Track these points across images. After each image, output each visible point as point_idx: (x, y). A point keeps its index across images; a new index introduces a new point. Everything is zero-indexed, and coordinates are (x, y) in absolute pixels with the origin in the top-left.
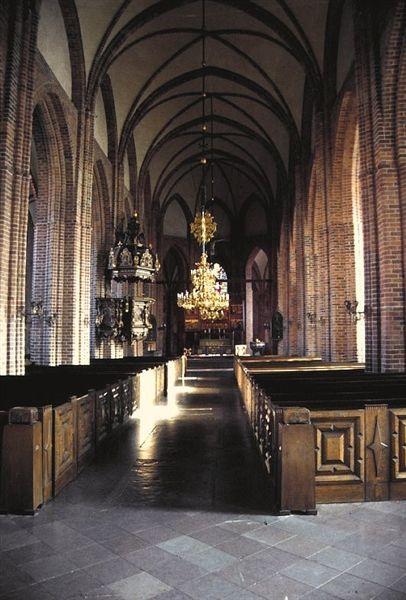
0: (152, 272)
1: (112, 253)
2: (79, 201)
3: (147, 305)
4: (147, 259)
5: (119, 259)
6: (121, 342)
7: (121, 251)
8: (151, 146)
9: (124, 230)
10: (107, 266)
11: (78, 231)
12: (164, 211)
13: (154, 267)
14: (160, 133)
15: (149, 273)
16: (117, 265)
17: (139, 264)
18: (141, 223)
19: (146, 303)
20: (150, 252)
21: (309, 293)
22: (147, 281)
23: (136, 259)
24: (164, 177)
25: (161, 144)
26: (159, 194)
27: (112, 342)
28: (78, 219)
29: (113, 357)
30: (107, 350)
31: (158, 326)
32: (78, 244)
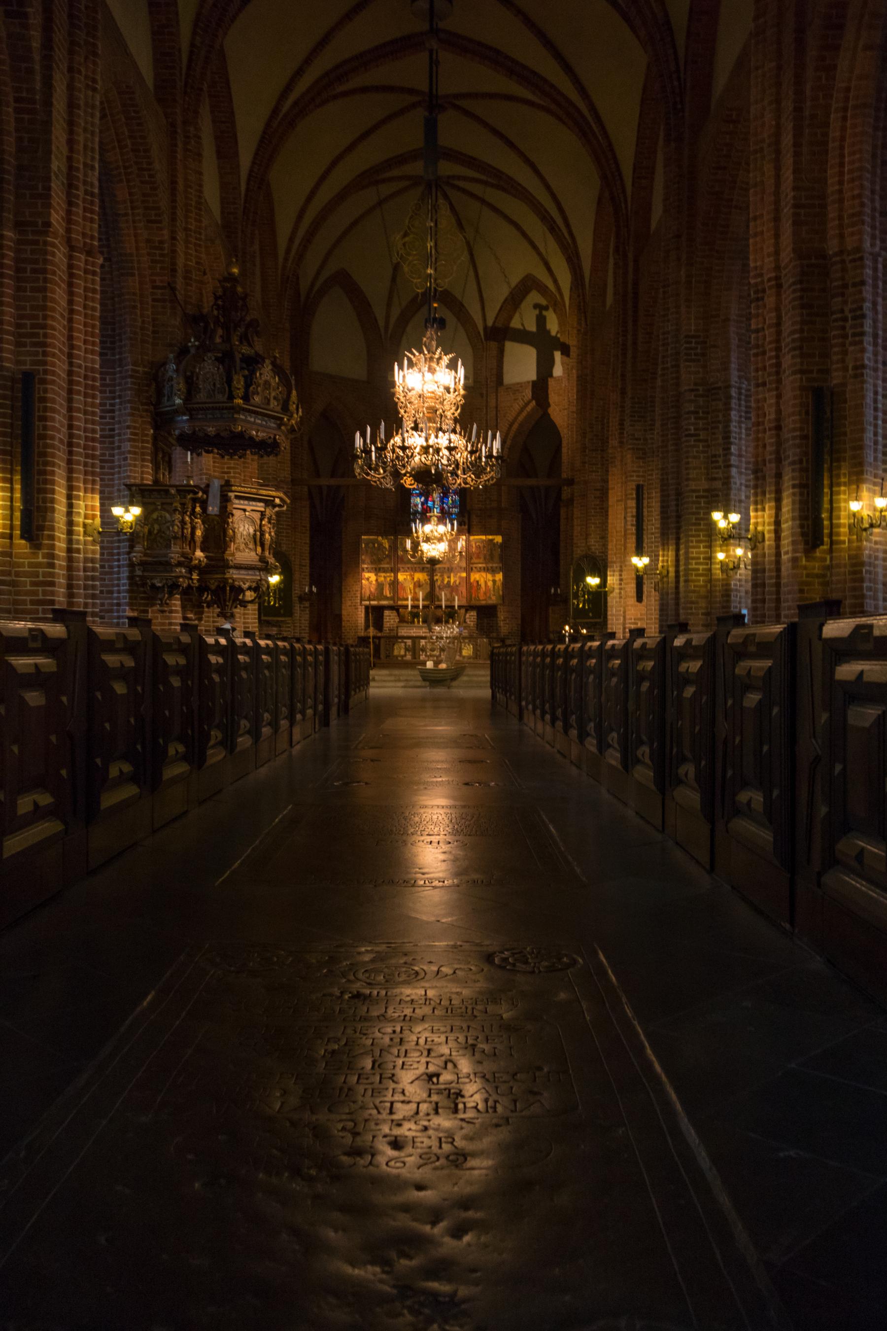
2: (57, 164)
3: (269, 512)
4: (267, 383)
8: (275, 111)
11: (59, 255)
14: (299, 72)
17: (246, 398)
20: (277, 369)
22: (267, 448)
23: (239, 382)
24: (301, 232)
28: (56, 218)
31: (296, 591)
32: (59, 295)
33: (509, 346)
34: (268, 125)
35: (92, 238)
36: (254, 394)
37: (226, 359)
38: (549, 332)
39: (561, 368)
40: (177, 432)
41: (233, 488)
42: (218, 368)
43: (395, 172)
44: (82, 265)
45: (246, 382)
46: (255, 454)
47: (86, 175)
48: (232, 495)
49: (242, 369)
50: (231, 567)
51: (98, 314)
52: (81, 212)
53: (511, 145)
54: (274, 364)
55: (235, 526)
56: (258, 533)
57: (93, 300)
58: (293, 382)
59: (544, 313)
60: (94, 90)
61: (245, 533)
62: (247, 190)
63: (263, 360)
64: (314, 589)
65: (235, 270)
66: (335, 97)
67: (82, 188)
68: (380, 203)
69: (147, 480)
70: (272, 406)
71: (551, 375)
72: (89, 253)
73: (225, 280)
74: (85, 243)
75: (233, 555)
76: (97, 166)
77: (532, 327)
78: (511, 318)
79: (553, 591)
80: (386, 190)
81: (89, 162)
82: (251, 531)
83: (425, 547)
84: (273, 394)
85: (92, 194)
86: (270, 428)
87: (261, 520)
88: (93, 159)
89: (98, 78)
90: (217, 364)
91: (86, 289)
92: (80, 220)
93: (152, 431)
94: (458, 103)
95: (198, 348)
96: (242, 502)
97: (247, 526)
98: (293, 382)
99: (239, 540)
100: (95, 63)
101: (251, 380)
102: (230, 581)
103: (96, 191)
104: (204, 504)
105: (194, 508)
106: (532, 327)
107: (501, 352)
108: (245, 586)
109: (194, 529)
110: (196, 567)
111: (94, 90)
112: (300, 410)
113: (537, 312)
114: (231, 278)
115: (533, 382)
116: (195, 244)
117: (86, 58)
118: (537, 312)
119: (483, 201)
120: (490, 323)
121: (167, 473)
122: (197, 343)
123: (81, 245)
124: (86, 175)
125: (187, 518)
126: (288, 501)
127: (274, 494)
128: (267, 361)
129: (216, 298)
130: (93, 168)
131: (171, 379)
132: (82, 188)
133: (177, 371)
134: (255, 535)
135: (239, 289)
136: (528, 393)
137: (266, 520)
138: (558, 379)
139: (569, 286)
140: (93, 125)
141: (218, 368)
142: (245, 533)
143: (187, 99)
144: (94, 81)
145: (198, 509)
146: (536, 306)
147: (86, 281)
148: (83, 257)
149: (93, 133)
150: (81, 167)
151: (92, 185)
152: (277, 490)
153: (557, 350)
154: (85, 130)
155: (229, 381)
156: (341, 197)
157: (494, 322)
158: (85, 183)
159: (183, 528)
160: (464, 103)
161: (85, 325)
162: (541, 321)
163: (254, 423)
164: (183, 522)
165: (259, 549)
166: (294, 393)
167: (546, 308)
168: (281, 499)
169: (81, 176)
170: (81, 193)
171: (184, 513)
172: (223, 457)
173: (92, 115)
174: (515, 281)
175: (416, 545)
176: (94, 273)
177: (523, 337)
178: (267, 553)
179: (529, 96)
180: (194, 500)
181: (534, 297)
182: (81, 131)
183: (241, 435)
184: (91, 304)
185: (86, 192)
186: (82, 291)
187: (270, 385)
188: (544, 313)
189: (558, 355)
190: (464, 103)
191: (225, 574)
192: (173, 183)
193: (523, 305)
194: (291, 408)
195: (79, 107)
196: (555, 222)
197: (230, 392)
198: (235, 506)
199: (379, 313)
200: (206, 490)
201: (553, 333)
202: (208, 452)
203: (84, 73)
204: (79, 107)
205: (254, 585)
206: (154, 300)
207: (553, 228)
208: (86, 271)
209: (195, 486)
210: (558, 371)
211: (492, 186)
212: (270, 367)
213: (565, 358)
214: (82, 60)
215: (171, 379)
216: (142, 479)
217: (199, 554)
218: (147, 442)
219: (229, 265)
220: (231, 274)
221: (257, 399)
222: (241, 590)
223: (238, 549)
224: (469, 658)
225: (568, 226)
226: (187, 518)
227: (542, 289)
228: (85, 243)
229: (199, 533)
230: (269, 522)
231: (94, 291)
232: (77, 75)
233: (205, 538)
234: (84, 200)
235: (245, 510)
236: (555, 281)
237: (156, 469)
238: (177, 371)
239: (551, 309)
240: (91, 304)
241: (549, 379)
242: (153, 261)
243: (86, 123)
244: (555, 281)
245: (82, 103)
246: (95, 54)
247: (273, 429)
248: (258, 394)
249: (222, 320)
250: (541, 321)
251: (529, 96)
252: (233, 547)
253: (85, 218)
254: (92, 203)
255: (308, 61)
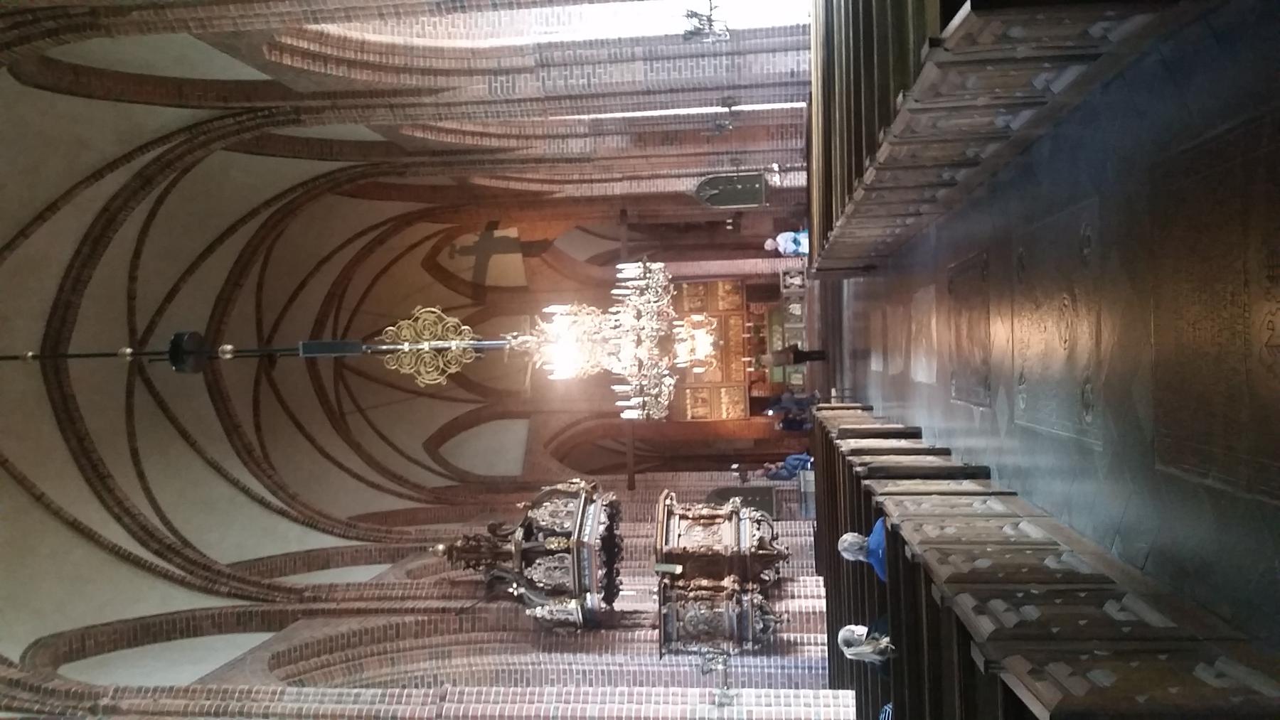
0: (589, 501)
1: (539, 612)
3: (678, 510)
5: (558, 592)
6: (779, 583)
7: (531, 584)
8: (282, 513)
9: (479, 577)
10: (574, 624)
12: (464, 478)
13: (575, 495)
14: (246, 491)
15: (591, 508)
16: (572, 596)
17: (568, 535)
18: (458, 531)
19: (670, 514)
20: (536, 505)
21: (640, 77)
22: (614, 514)
23: (553, 544)
25: (278, 488)
26: (416, 487)
27: (779, 607)
29: (822, 605)
30: (806, 618)
31: (738, 484)
33: (489, 282)
34: (295, 520)
35: (426, 695)
36: (563, 528)
37: (528, 557)
38: (476, 243)
39: (510, 229)
40: (603, 605)
41: (659, 547)
42: (539, 564)
43: (332, 397)
44: (454, 706)
45: (550, 535)
46: (617, 526)
47: (365, 702)
48: (664, 551)
49: (537, 539)
50: (739, 548)
51: (502, 689)
52: (401, 708)
53: (302, 285)
54: (532, 508)
55: (696, 544)
56: (702, 521)
57: (488, 694)
58: (548, 488)
59: (458, 247)
60: (282, 693)
61: (702, 535)
62: (357, 539)
63: (527, 518)
64: (735, 466)
65: (441, 547)
66: (266, 456)
67: (376, 707)
68: (361, 410)
69: (652, 636)
70: (573, 509)
71: (517, 239)
72: (443, 699)
73: (450, 558)
74: (432, 703)
75: (726, 548)
76: (356, 691)
77: (471, 260)
78: (463, 281)
79: (729, 227)
80: (348, 406)
81: (352, 698)
82: (699, 528)
83: (700, 355)
84: (562, 508)
85: (384, 695)
86: (595, 511)
87: (687, 518)
88: (349, 695)
89: (271, 689)
90: (534, 565)
91: (478, 702)
92: (410, 708)
93: (603, 631)
94: (266, 336)
95: (519, 585)
96: (671, 538)
97: (695, 533)
98: (548, 488)
99: (709, 542)
100: (257, 692)
101: (548, 529)
102: (753, 550)
103: (380, 691)
104: (674, 577)
105: (680, 588)
106: (471, 260)
107: (496, 289)
108: (758, 534)
109: (701, 588)
110: (740, 585)
111: (282, 693)
112: (574, 480)
113: (457, 256)
114: (449, 552)
115: (524, 255)
116: (417, 589)
117: (254, 700)
118: (457, 256)
119: (355, 312)
120: (469, 301)
121: (643, 616)
122: (515, 585)
123: (435, 707)
124: (365, 702)
125: (692, 594)
126: (666, 491)
127: (661, 505)
128: (530, 514)
129: (468, 567)
130: (358, 695)
131: (551, 612)
132: (376, 707)
133: (543, 606)
134: (704, 525)
135: (459, 543)
136: (535, 261)
137: (688, 513)
138: (520, 233)
139: (431, 225)
140: (315, 695)
141: (539, 564)
142: (702, 535)
143: (278, 599)
144: (274, 693)
145: (681, 583)
146: (451, 257)
147: (470, 702)
148: (446, 705)
149: (324, 695)
150: (357, 706)
151: (374, 696)
152: (657, 502)
153: (492, 235)
154: (321, 702)
155: (552, 552)
156: (357, 448)
157: (467, 297)
158: (373, 703)
159: (702, 599)
160: (267, 330)
161: (514, 702)
162: (465, 251)
163: (592, 526)
164: (696, 599)
165: (718, 520)
166: (559, 486)
167: (453, 246)
168: (666, 498)
169: (366, 707)
170: (383, 707)
171: (686, 599)
172: (622, 558)
173: (307, 695)
174: (428, 278)
175: (701, 363)
176: (462, 693)
177: (481, 268)
178: (720, 512)
179: (256, 269)
180: (672, 587)
181: (443, 259)
182: (323, 706)
183: (603, 539)
184: (492, 697)
185: (382, 702)
186: (481, 706)
187: (553, 511)
188: (458, 247)
189: (498, 233)
190: (267, 330)
191: (746, 556)
192: (359, 612)
193: (451, 269)
194: (574, 490)
195: (301, 709)
196: (373, 240)
197: (562, 551)
198: (676, 546)
199: (461, 410)
200: (664, 575)
201: (477, 238)
202: (618, 574)
203: (267, 703)
204: (301, 709)
205: (756, 525)
206: (473, 630)
207: (380, 241)
208: (460, 702)
209: (660, 586)
210: (512, 232)
211: (340, 303)
212: (535, 511)
213: (500, 226)
214: (255, 704)
215: (551, 612)
216: (652, 641)
217: (727, 582)
218: (614, 636)
219: (435, 553)
220: (444, 553)
221: (567, 524)
222: (761, 539)
223: (720, 542)
224: (802, 308)
225: (376, 227)
226: (692, 594)
227: (436, 250)
228: (432, 703)
229: (704, 583)
230: (689, 510)
231: (479, 693)
232: (271, 710)
233: (708, 576)
234: (390, 703)
235: (679, 536)
236: (428, 238)
237: (642, 626)
238: (543, 606)
239: (454, 242)
240: (492, 697)
241: (522, 240)
242: (436, 631)
243: (314, 701)
244: (428, 238)
245: (296, 706)
246: (250, 692)
247: (595, 507)
248: (562, 523)
249: (489, 561)
250: (465, 251)
251: (256, 269)
252: (717, 547)
253: (408, 703)
254: (392, 696)
255: (235, 483)
